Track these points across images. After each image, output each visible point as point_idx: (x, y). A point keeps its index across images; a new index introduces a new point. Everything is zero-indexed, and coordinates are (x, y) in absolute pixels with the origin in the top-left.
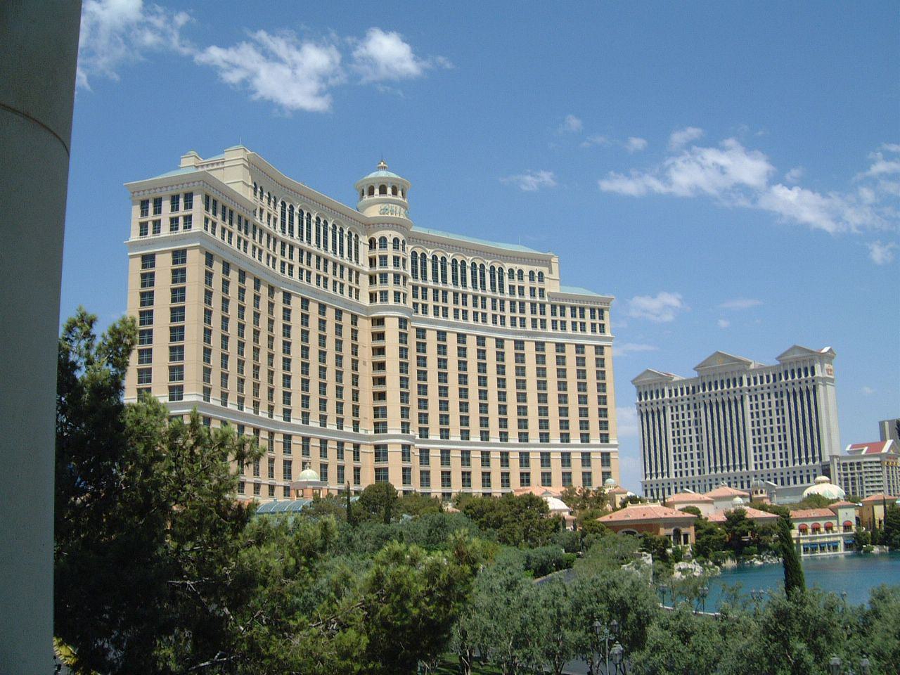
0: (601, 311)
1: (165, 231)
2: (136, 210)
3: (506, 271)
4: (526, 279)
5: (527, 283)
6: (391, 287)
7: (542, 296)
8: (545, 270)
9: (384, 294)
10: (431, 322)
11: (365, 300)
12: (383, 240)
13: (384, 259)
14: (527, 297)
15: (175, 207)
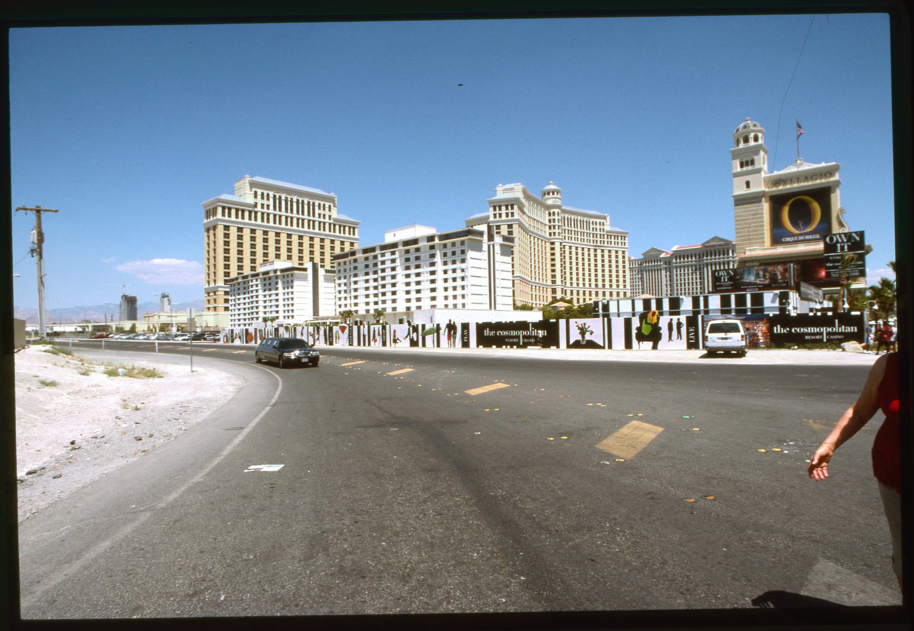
0: (625, 237)
1: (504, 217)
2: (492, 209)
3: (591, 222)
4: (598, 225)
5: (598, 227)
6: (557, 231)
7: (603, 231)
8: (604, 221)
9: (554, 233)
10: (574, 243)
11: (547, 235)
12: (554, 213)
13: (554, 220)
14: (598, 232)
15: (507, 209)
